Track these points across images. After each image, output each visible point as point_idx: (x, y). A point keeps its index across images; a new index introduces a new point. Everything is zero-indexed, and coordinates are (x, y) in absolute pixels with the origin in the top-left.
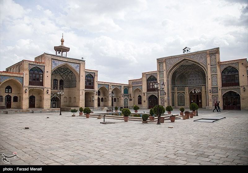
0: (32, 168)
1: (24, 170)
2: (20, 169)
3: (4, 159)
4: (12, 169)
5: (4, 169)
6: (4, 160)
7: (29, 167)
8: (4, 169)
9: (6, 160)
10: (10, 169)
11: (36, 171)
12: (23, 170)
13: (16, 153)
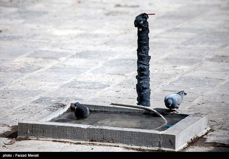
0: (29, 155)
1: (22, 156)
2: (19, 156)
3: (3, 146)
4: (11, 156)
5: (4, 156)
7: (27, 153)
8: (4, 156)
9: (6, 147)
10: (9, 156)
11: (34, 157)
12: (21, 156)
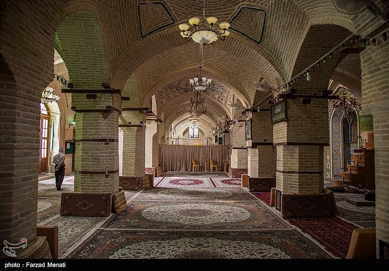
0: (50, 263)
1: (38, 266)
2: (32, 265)
3: (5, 249)
4: (18, 265)
5: (7, 265)
6: (6, 251)
8: (7, 265)
9: (10, 251)
10: (16, 265)
12: (36, 266)
13: (25, 240)
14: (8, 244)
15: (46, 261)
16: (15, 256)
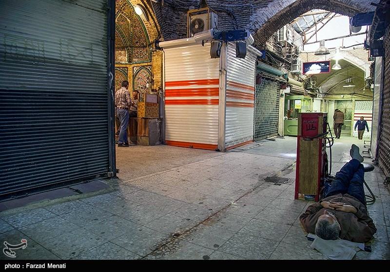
0: (50, 264)
1: (38, 267)
2: (32, 266)
3: (5, 250)
4: (18, 266)
5: (7, 266)
8: (7, 266)
10: (16, 266)
11: (57, 269)
12: (36, 267)
13: (25, 241)
14: (8, 245)
15: (46, 262)
16: (16, 257)
